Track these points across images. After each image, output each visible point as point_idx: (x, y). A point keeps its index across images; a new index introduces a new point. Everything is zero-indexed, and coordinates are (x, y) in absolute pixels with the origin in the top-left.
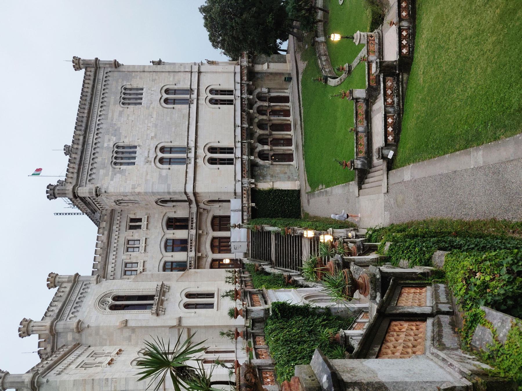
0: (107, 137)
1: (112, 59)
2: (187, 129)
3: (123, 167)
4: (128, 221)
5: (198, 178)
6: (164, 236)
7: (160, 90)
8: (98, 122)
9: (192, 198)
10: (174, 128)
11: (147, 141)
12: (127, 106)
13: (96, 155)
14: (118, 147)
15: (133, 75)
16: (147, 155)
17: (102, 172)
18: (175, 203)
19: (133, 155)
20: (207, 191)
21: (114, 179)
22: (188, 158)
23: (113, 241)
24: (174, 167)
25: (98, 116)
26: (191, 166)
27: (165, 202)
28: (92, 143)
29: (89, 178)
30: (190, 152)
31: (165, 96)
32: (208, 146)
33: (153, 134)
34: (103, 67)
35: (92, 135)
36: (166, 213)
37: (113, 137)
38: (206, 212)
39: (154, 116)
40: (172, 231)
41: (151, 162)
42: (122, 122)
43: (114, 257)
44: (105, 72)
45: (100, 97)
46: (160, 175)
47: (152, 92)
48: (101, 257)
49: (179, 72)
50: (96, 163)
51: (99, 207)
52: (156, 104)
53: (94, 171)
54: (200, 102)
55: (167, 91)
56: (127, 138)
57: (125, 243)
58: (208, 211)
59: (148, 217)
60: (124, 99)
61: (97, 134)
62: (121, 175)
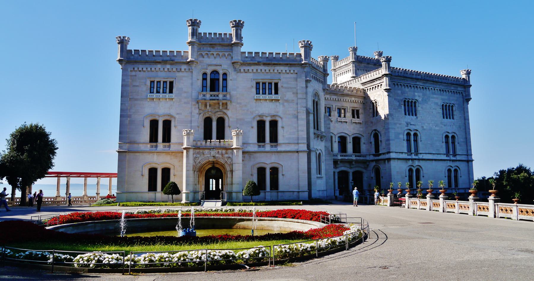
0: (421, 94)
1: (471, 97)
2: (430, 152)
3: (403, 106)
4: (358, 109)
5: (399, 161)
7: (454, 131)
11: (420, 124)
13: (410, 88)
14: (415, 103)
16: (411, 123)
17: (399, 92)
19: (411, 114)
20: (392, 168)
21: (395, 101)
22: (412, 153)
23: (345, 98)
24: (405, 143)
25: (434, 88)
26: (405, 156)
27: (376, 136)
29: (396, 83)
30: (415, 155)
31: (450, 136)
32: (420, 168)
33: (425, 127)
35: (422, 84)
36: (363, 136)
37: (421, 98)
39: (437, 128)
40: (351, 141)
41: (407, 126)
42: (431, 105)
43: (334, 99)
46: (400, 134)
47: (452, 126)
48: (334, 89)
49: (467, 145)
50: (405, 87)
52: (445, 129)
53: (400, 87)
54: (448, 162)
55: (453, 137)
56: (421, 109)
58: (366, 168)
59: (361, 123)
60: (446, 105)
61: (423, 88)
62: (398, 105)
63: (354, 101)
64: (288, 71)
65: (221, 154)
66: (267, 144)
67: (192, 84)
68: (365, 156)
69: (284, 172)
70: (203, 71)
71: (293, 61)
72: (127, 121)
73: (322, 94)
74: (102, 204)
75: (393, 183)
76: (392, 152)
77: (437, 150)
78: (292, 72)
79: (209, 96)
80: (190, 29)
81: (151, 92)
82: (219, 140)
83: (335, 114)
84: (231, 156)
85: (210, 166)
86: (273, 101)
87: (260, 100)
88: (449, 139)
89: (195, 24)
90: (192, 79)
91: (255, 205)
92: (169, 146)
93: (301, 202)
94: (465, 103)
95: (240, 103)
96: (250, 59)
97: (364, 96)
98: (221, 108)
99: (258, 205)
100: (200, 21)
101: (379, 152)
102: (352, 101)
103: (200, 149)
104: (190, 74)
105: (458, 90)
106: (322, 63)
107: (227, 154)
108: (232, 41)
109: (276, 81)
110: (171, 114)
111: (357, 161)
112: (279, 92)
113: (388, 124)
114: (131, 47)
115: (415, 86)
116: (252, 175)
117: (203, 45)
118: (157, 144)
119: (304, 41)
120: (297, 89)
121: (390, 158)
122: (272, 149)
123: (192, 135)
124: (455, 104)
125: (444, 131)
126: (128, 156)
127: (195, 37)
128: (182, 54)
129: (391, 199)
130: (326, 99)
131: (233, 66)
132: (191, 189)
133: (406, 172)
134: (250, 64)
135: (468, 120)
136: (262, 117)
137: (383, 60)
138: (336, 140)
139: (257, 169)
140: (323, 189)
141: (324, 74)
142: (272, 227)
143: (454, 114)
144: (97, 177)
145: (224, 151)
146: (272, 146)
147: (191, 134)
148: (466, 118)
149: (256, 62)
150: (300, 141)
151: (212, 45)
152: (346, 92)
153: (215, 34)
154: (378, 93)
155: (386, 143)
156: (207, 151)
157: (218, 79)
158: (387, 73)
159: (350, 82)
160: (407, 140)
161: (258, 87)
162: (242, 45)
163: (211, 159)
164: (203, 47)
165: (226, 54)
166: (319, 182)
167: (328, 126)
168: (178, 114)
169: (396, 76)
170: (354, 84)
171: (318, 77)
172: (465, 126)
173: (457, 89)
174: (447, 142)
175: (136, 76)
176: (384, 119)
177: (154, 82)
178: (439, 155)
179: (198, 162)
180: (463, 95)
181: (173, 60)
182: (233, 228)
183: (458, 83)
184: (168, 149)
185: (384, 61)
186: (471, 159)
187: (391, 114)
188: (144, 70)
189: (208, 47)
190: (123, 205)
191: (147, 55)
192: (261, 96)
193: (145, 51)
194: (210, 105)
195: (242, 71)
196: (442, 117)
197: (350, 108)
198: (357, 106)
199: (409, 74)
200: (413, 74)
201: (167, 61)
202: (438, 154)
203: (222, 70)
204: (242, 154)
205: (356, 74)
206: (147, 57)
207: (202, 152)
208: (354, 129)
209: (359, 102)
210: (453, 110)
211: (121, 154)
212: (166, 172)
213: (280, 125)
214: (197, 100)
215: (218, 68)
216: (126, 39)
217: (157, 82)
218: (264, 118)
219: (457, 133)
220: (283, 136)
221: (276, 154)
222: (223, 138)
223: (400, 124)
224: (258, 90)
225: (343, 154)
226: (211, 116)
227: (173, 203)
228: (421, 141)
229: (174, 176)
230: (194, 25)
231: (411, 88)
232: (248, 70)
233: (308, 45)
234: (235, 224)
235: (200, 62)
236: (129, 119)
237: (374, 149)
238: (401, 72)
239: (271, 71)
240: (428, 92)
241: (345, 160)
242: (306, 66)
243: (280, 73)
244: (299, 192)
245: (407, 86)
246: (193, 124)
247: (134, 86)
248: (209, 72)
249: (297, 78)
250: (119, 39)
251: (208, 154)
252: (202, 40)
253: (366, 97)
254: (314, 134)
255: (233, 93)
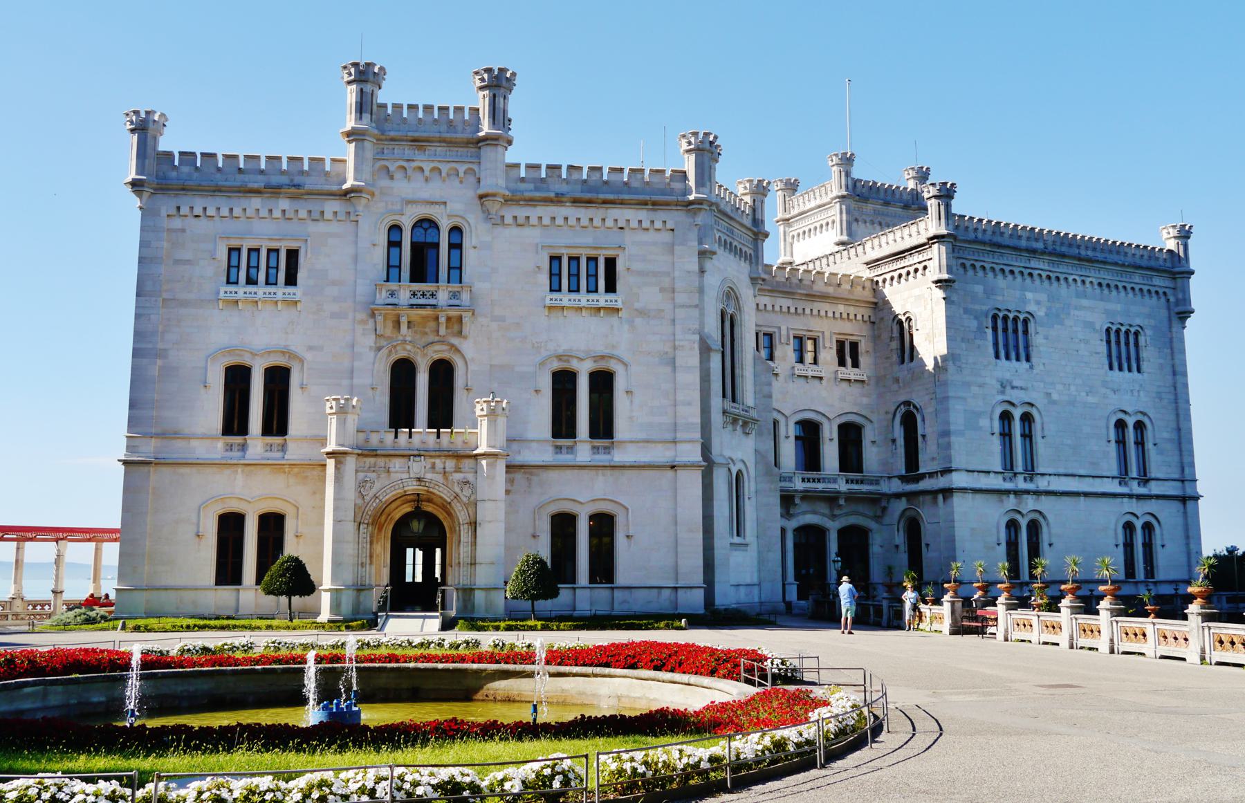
0: (1043, 297)
1: (1194, 306)
2: (1070, 472)
3: (989, 332)
5: (978, 496)
6: (828, 419)
7: (1141, 409)
8: (1070, 278)
9: (925, 485)
10: (1069, 442)
11: (1042, 385)
12: (1105, 339)
13: (1010, 277)
14: (1026, 321)
15: (1166, 350)
16: (1015, 384)
17: (979, 289)
18: (903, 443)
19: (1013, 355)
20: (956, 517)
21: (965, 316)
22: (1015, 474)
23: (817, 306)
24: (996, 444)
26: (996, 482)
27: (909, 422)
28: (1032, 268)
29: (968, 264)
30: (1025, 479)
31: (1131, 421)
32: (1041, 520)
33: (1055, 396)
34: (1176, 283)
35: (1046, 267)
36: (871, 422)
38: (879, 513)
39: (1091, 399)
40: (835, 435)
41: (1003, 393)
43: (785, 309)
44: (1166, 290)
45: (1120, 281)
46: (979, 415)
47: (1136, 394)
48: (784, 280)
49: (1180, 450)
50: (995, 275)
51: (888, 276)
53: (981, 273)
54: (1126, 500)
55: (1139, 426)
56: (1044, 341)
57: (811, 331)
58: (878, 518)
59: (863, 381)
60: (1118, 331)
61: (1049, 277)
63: (845, 316)
64: (646, 224)
65: (442, 470)
66: (580, 441)
67: (356, 258)
68: (876, 481)
69: (631, 527)
70: (388, 222)
71: (663, 193)
72: (154, 369)
73: (747, 294)
74: (69, 624)
75: (959, 565)
76: (956, 470)
77: (1092, 464)
78: (658, 225)
79: (408, 294)
80: (351, 93)
81: (228, 282)
82: (435, 430)
83: (785, 352)
84: (470, 477)
85: (407, 509)
86: (602, 311)
87: (563, 307)
88: (1126, 430)
89: (365, 76)
90: (356, 243)
91: (544, 628)
92: (283, 446)
93: (683, 620)
94: (1176, 325)
95: (502, 319)
96: (531, 186)
97: (875, 300)
98: (443, 331)
99: (553, 630)
100: (382, 69)
101: (918, 469)
102: (837, 315)
103: (376, 455)
104: (350, 227)
105: (1155, 286)
106: (748, 199)
107: (461, 472)
108: (478, 130)
109: (610, 253)
110: (293, 348)
111: (851, 497)
112: (619, 286)
113: (945, 384)
114: (170, 142)
115: (1026, 272)
116: (534, 536)
117: (392, 140)
118: (245, 439)
119: (695, 134)
120: (674, 278)
121: (952, 489)
122: (597, 457)
123: (353, 413)
124: (1144, 327)
125: (1111, 408)
126: (156, 477)
127: (366, 117)
128: (328, 168)
129: (953, 612)
130: (762, 307)
131: (482, 204)
132: (349, 578)
133: (998, 532)
134: (531, 200)
135: (1185, 374)
136: (568, 361)
137: (931, 195)
138: (789, 432)
139: (549, 519)
140: (748, 581)
141: (756, 234)
142: (593, 695)
143: (1141, 356)
144: (57, 541)
145: (450, 464)
146: (595, 449)
147: (350, 410)
148: (1178, 369)
149: (552, 195)
150: (679, 436)
151: (418, 142)
152: (819, 287)
153: (428, 108)
154: (916, 292)
155: (940, 441)
156: (397, 464)
157: (436, 246)
158: (943, 231)
159: (831, 258)
160: (1003, 435)
161: (556, 271)
162: (510, 142)
163: (412, 487)
164: (391, 147)
165: (462, 169)
166: (737, 557)
167: (766, 389)
168: (310, 348)
169: (970, 242)
170: (844, 265)
171: (735, 243)
172: (1176, 395)
173: (1150, 283)
174: (1121, 442)
175: (183, 231)
176: (934, 369)
177: (239, 250)
178: (1098, 480)
179: (371, 495)
180: (1168, 300)
181: (298, 186)
182: (475, 697)
183: (1153, 263)
184: (279, 454)
185: (935, 197)
186: (1193, 494)
187: (953, 354)
188: (208, 214)
189: (407, 148)
190: (137, 629)
191: (219, 169)
192: (565, 298)
193: (213, 155)
194: (409, 322)
195: (508, 220)
196: (1107, 367)
197: (831, 338)
198: (854, 330)
199: (1006, 235)
200: (1020, 237)
201: (280, 187)
202: (1093, 477)
203: (448, 216)
204: (507, 472)
205: (850, 234)
206: (218, 176)
207: (383, 465)
208: (842, 399)
209: (859, 317)
210: (1140, 345)
211: (133, 468)
212: (272, 525)
213: (620, 385)
214: (372, 306)
215: (434, 212)
216: (156, 118)
217: (250, 250)
218: (574, 365)
219: (1150, 415)
220: (631, 418)
221: (608, 472)
222: (448, 423)
223: (980, 386)
224: (555, 279)
225: (809, 476)
226: (412, 356)
227: (291, 620)
228: (1043, 437)
229: (295, 540)
230: (366, 81)
231: (1015, 278)
232: (528, 218)
233: (707, 146)
234: (481, 688)
235: (381, 193)
236: (159, 362)
237: (903, 460)
238: (985, 231)
239: (597, 222)
240: (1063, 290)
241: (816, 492)
242: (700, 209)
243: (621, 228)
244: (676, 588)
245: (1003, 271)
246: (355, 381)
247: (177, 262)
248: (407, 223)
249: (673, 245)
250: (134, 118)
251: (403, 472)
252: (387, 126)
253: (879, 305)
254: (724, 412)
255: (480, 286)
